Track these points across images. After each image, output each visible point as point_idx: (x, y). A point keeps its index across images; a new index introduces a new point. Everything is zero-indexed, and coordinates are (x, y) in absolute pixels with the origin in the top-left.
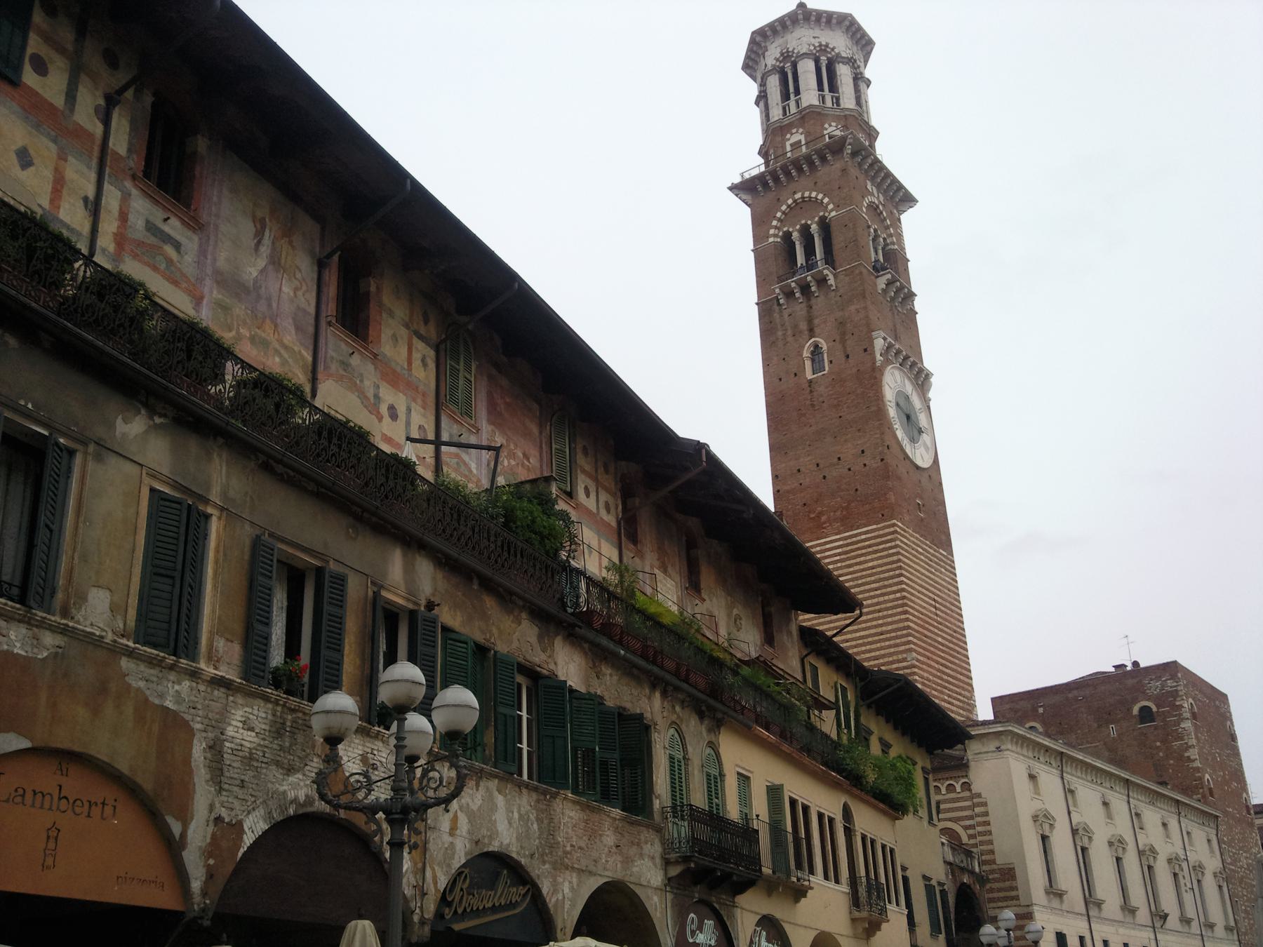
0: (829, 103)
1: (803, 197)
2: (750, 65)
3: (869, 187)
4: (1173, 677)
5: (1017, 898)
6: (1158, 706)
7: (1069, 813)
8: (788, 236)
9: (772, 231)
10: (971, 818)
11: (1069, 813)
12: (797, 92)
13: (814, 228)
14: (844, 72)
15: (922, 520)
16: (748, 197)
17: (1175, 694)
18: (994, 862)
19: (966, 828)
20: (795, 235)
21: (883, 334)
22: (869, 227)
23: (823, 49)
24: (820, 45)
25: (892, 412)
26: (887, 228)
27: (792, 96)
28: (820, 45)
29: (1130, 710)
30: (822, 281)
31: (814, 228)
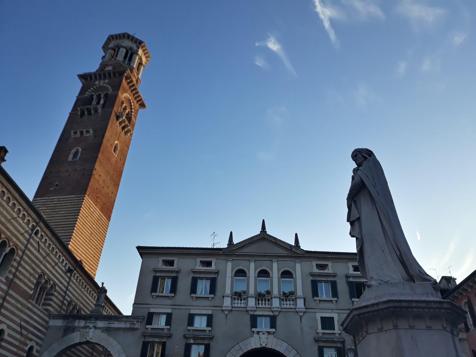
0: (126, 62)
1: (103, 86)
2: (105, 48)
8: (92, 96)
9: (87, 93)
12: (116, 56)
13: (102, 95)
16: (84, 81)
20: (95, 97)
22: (123, 103)
23: (131, 49)
24: (130, 47)
27: (114, 57)
28: (130, 47)
30: (96, 111)
31: (102, 95)
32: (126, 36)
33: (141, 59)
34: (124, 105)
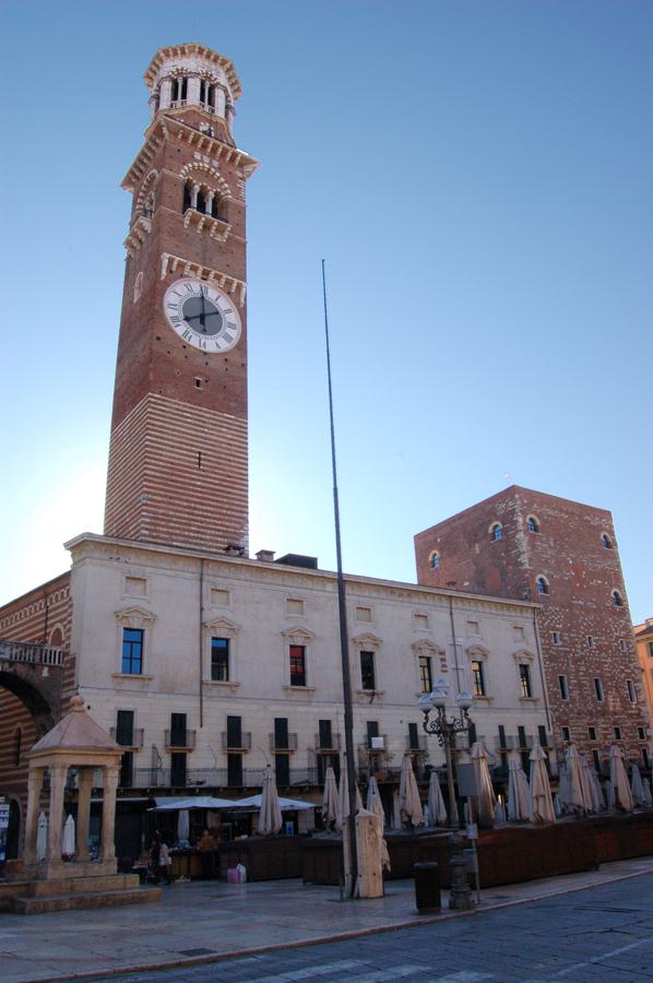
3: (197, 156)
4: (513, 499)
5: (72, 683)
6: (503, 524)
7: (202, 609)
10: (65, 619)
11: (202, 609)
14: (194, 87)
15: (200, 392)
17: (513, 512)
18: (67, 654)
19: (65, 626)
21: (168, 255)
24: (177, 70)
25: (170, 313)
26: (222, 183)
28: (177, 70)
29: (487, 530)
32: (162, 54)
33: (209, 77)
34: (197, 188)
